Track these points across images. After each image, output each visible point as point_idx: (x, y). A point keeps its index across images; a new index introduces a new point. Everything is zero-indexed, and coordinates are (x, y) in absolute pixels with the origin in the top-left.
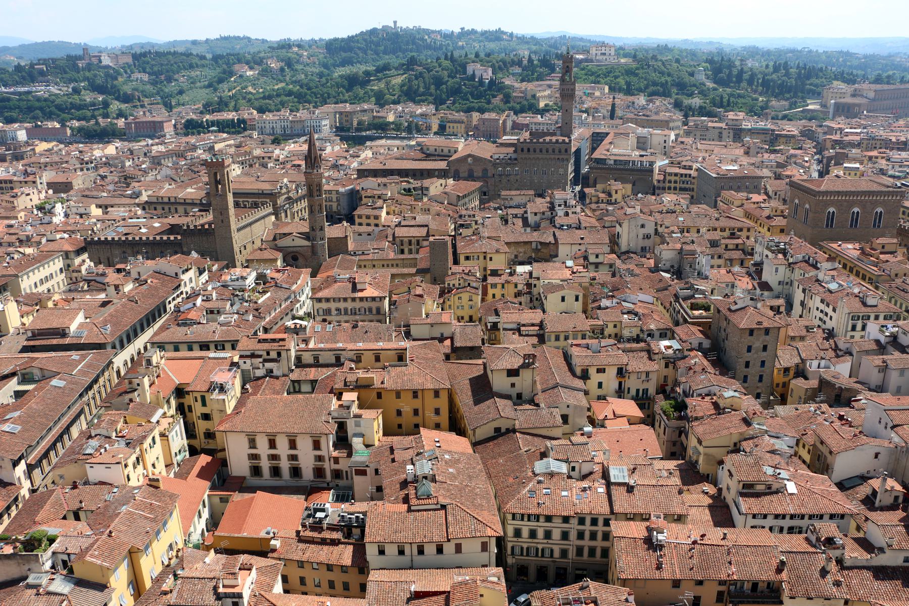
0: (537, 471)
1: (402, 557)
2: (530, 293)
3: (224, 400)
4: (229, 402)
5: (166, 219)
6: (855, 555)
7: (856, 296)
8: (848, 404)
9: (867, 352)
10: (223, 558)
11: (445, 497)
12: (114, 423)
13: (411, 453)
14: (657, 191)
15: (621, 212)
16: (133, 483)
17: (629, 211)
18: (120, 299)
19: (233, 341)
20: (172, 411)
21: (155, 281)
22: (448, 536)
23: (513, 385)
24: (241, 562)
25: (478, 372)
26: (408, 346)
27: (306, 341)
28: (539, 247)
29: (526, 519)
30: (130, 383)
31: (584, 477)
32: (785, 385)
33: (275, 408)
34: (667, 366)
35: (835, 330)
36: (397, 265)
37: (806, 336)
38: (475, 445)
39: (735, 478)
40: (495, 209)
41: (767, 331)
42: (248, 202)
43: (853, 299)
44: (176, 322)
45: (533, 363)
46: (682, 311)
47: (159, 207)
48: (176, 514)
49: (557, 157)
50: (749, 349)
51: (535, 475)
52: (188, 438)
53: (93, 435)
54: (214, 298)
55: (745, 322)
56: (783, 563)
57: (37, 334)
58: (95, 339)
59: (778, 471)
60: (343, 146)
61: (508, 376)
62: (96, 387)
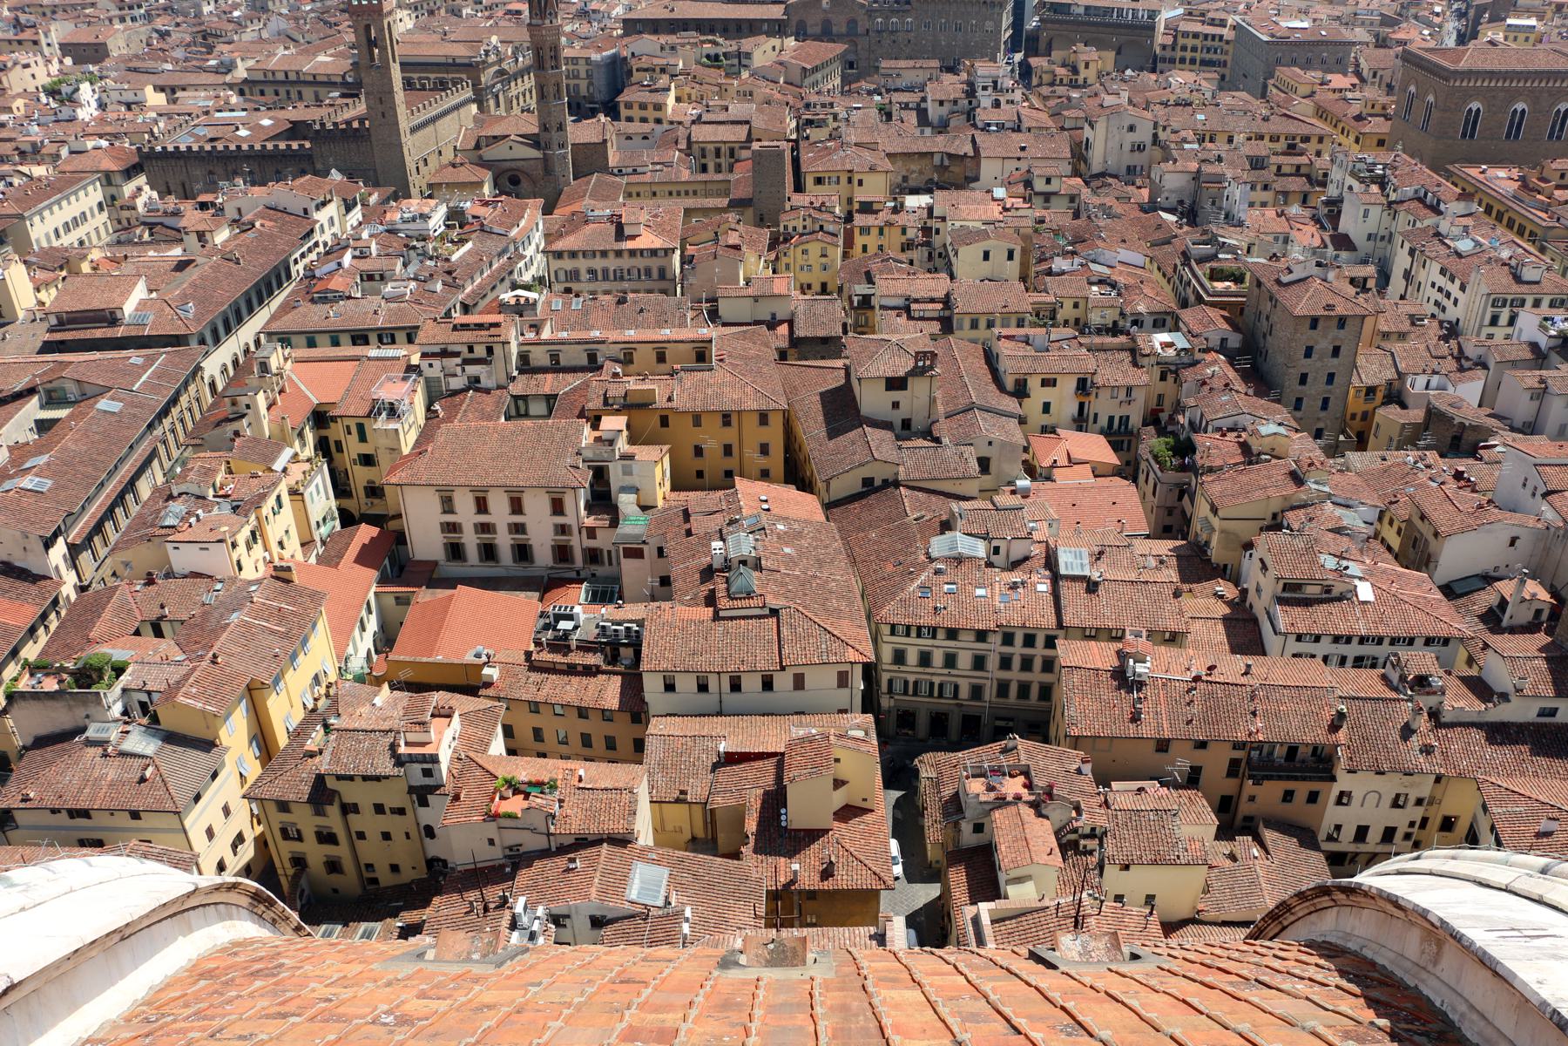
0: (935, 553)
1: (703, 696)
2: (928, 244)
3: (396, 430)
5: (283, 112)
6: (1461, 704)
7: (1504, 264)
8: (1473, 452)
9: (1514, 364)
11: (776, 595)
12: (209, 472)
13: (719, 521)
14: (1160, 66)
15: (1094, 102)
16: (248, 574)
17: (1109, 100)
19: (410, 328)
20: (309, 451)
21: (268, 224)
22: (781, 662)
23: (896, 405)
24: (434, 704)
25: (835, 381)
27: (536, 327)
28: (946, 162)
29: (914, 633)
30: (234, 404)
31: (1014, 565)
32: (1367, 416)
33: (485, 443)
34: (1163, 378)
35: (1461, 323)
36: (695, 193)
37: (1409, 333)
38: (828, 506)
39: (1272, 573)
40: (870, 93)
41: (1342, 322)
43: (1497, 268)
45: (931, 368)
46: (1193, 281)
47: (269, 90)
48: (322, 625)
50: (1309, 352)
51: (931, 560)
52: (337, 497)
53: (175, 494)
54: (374, 253)
55: (1304, 304)
56: (1341, 716)
57: (66, 321)
59: (1345, 563)
61: (888, 389)
62: (175, 411)
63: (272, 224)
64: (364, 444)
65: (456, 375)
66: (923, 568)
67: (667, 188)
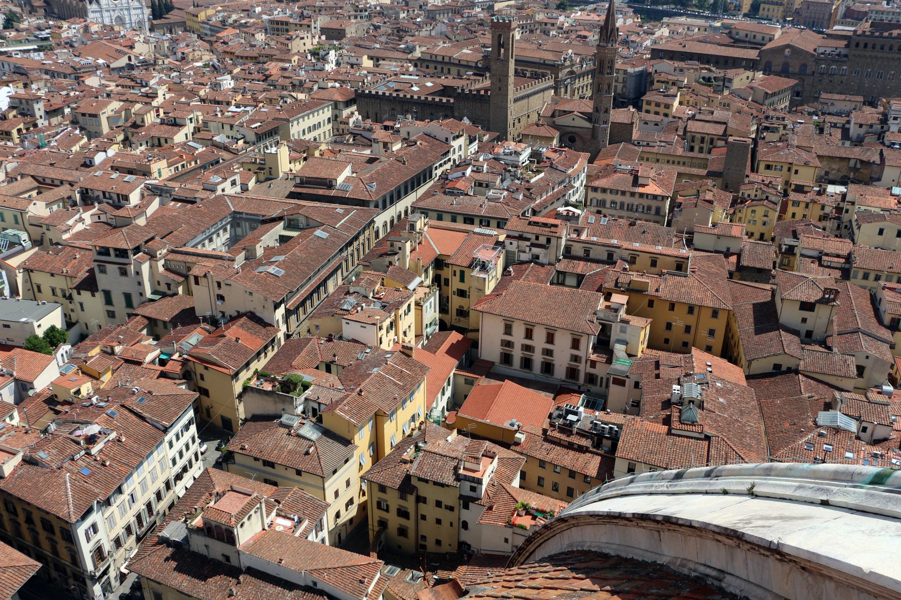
0: (820, 423)
2: (838, 218)
3: (485, 279)
10: (467, 441)
11: (711, 427)
12: (372, 283)
13: (676, 373)
16: (385, 346)
18: (388, 157)
19: (500, 218)
20: (428, 282)
21: (424, 144)
23: (804, 320)
24: (485, 448)
26: (691, 255)
27: (578, 232)
28: (858, 166)
30: (392, 245)
31: (876, 442)
36: (684, 164)
38: (748, 377)
40: (810, 114)
42: (527, 71)
44: (443, 190)
45: (834, 300)
47: (432, 66)
48: (423, 386)
51: (817, 426)
52: (440, 312)
53: (351, 291)
54: (485, 171)
57: (305, 182)
60: (636, 20)
62: (355, 244)
63: (426, 144)
64: (463, 284)
65: (525, 252)
66: (810, 430)
67: (667, 158)
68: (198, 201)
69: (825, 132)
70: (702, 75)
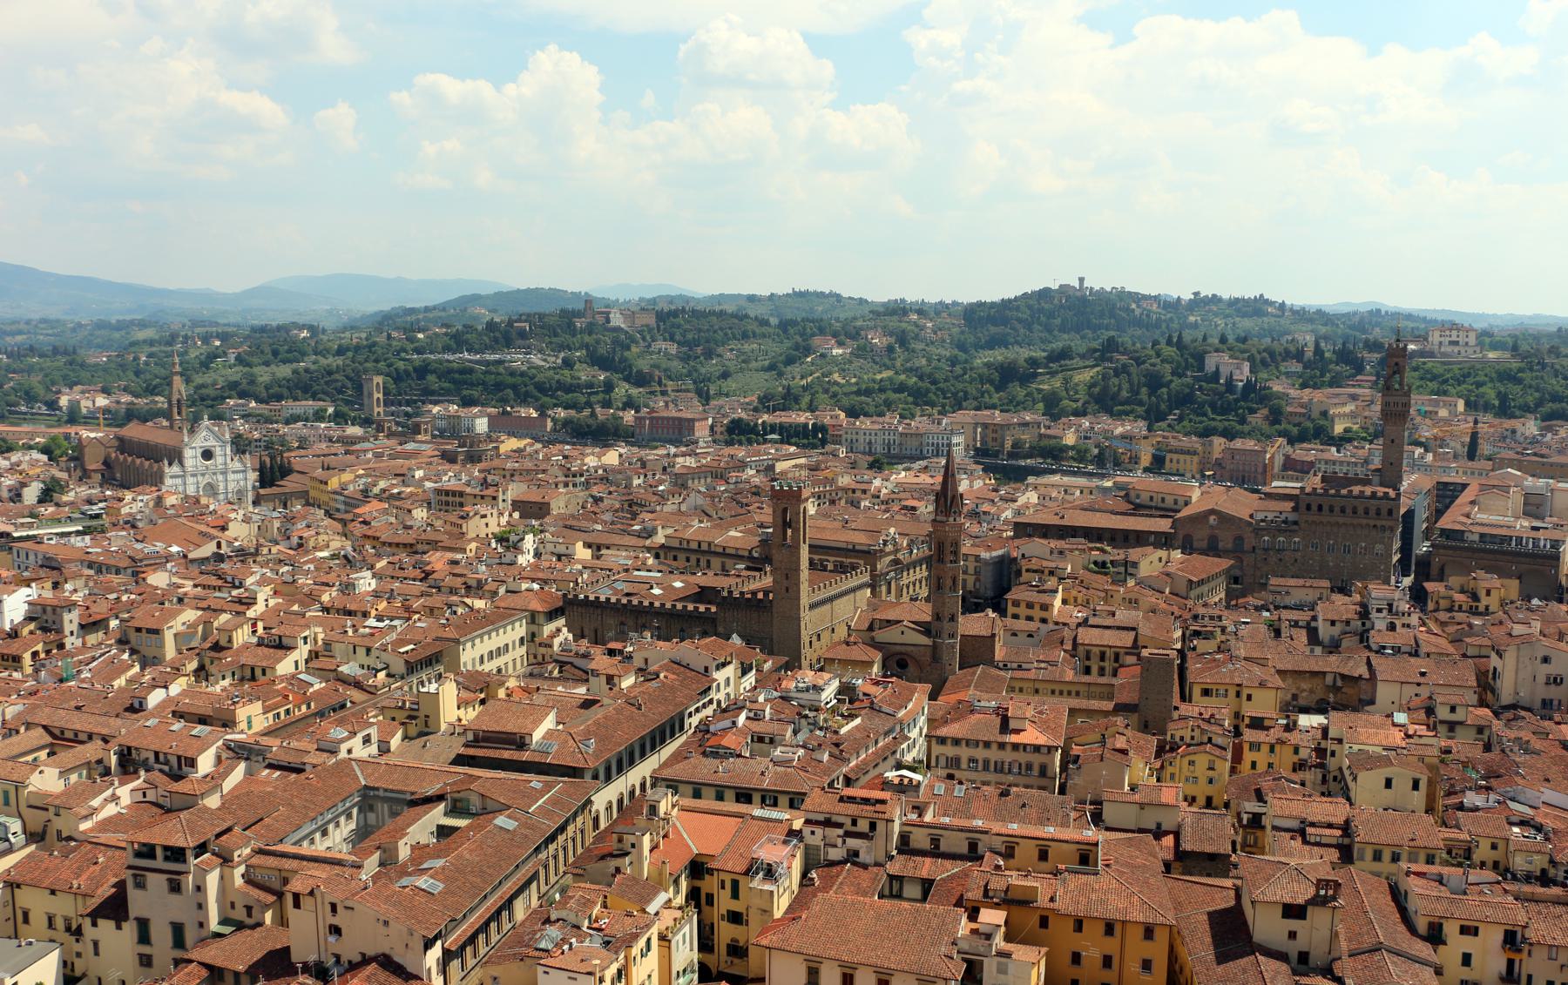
2: (1322, 766)
3: (772, 892)
4: (779, 897)
12: (589, 903)
15: (1498, 632)
17: (1518, 629)
18: (615, 699)
20: (680, 900)
21: (671, 676)
23: (1292, 935)
25: (1225, 901)
26: (1101, 838)
27: (920, 809)
30: (620, 841)
33: (860, 919)
36: (1078, 694)
40: (1258, 609)
44: (701, 749)
45: (1334, 898)
47: (682, 556)
49: (1372, 523)
52: (699, 951)
53: (553, 917)
54: (768, 717)
57: (482, 738)
58: (568, 759)
60: (987, 481)
62: (561, 838)
63: (674, 677)
65: (835, 846)
67: (1050, 687)
68: (308, 768)
69: (1283, 635)
70: (1092, 560)
